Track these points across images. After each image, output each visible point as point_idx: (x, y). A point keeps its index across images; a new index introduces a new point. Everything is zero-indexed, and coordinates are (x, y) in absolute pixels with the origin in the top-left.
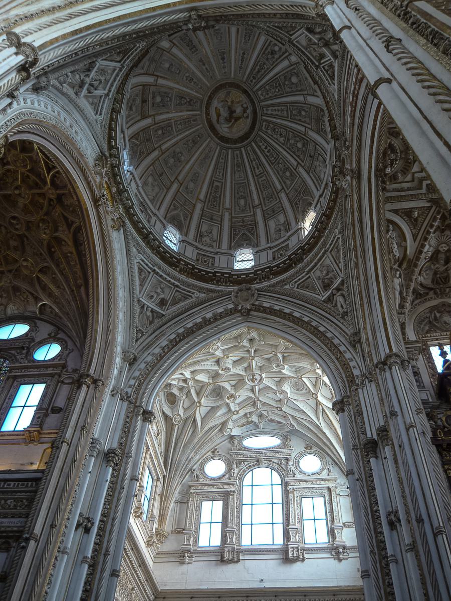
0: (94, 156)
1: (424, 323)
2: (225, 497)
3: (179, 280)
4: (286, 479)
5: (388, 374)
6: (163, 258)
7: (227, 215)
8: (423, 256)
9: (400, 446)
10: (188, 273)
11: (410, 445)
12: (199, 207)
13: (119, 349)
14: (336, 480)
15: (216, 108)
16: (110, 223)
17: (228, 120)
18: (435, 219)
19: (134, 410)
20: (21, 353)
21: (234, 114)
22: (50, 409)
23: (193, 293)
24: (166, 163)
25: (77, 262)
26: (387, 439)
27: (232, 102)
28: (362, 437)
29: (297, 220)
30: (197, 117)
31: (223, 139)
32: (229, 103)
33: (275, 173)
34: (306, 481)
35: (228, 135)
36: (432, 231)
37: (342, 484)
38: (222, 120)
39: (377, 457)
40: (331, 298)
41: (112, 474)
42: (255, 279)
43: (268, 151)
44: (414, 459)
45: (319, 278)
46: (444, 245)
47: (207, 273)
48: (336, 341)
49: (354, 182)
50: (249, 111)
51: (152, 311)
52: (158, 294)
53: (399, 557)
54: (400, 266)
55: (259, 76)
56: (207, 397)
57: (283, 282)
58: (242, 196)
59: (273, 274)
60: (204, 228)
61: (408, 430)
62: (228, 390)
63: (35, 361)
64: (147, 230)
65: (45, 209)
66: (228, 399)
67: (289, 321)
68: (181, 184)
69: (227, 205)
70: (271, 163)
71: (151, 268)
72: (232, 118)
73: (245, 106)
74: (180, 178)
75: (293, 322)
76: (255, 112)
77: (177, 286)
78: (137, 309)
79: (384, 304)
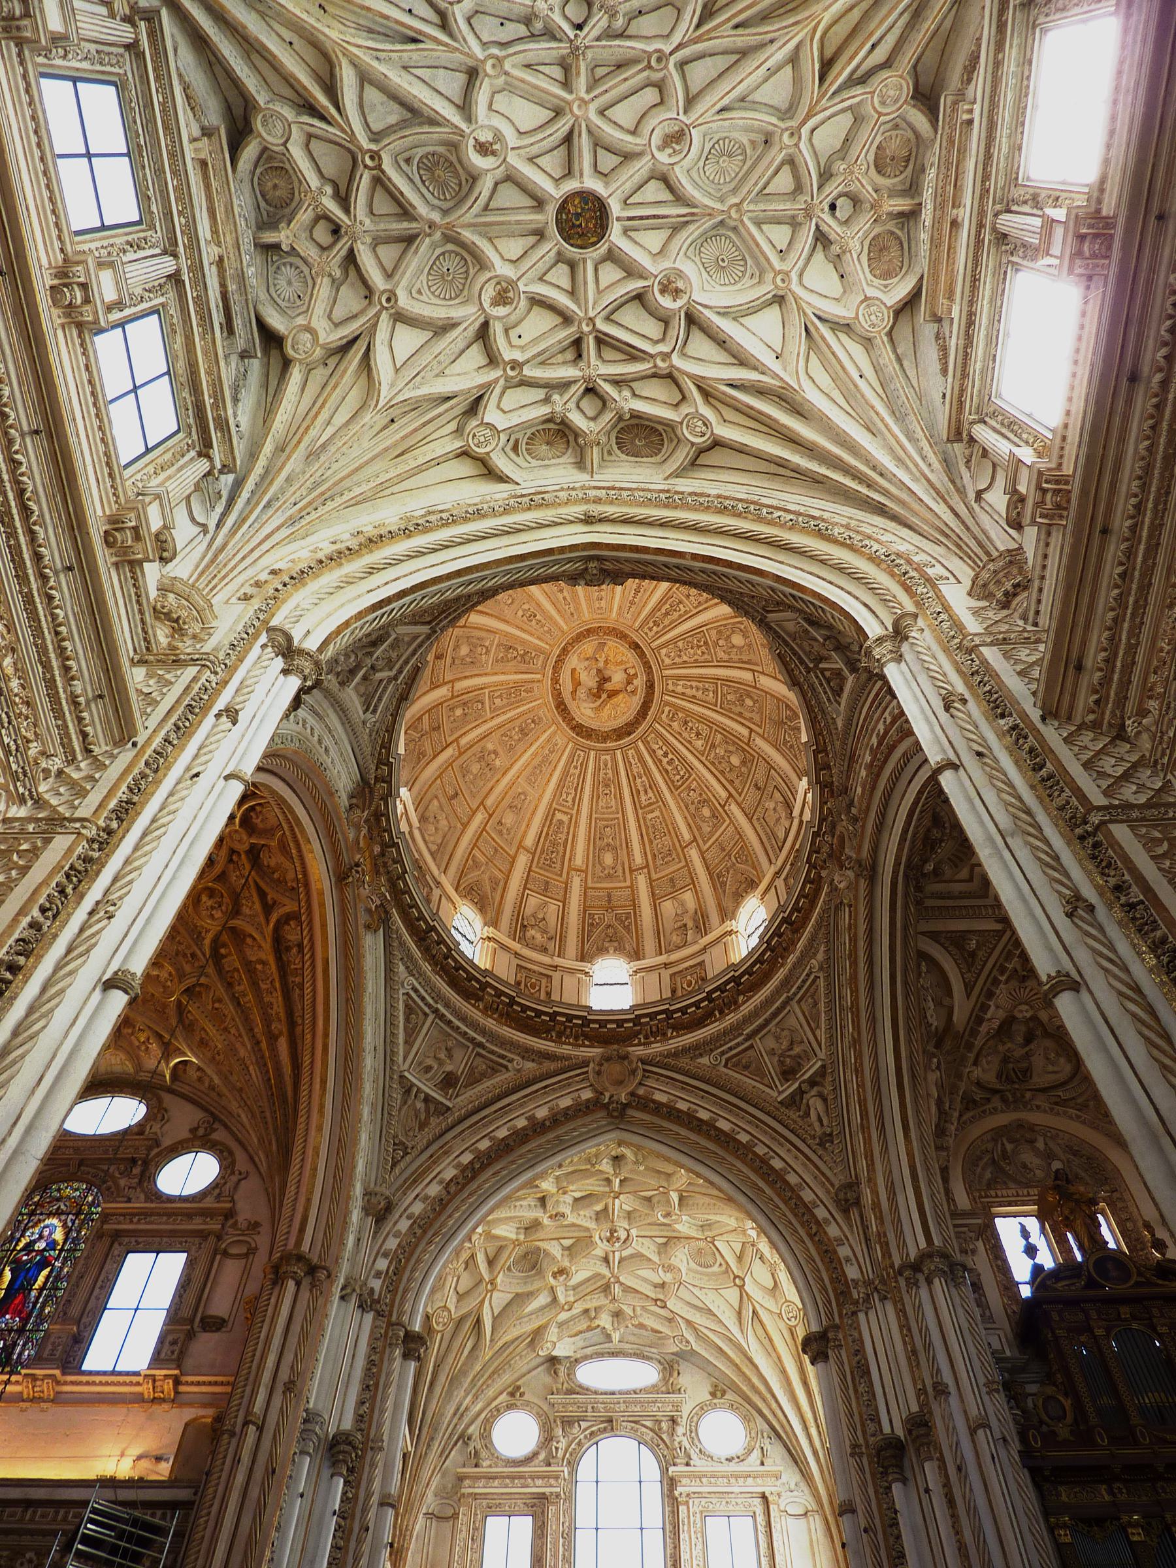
0: (350, 786)
1: (981, 1164)
2: (538, 1507)
4: (671, 1469)
5: (924, 1293)
6: (453, 983)
7: (576, 883)
8: (983, 1029)
9: (959, 1469)
10: (501, 1015)
11: (980, 1466)
12: (522, 860)
13: (358, 1189)
14: (778, 1476)
15: (573, 671)
16: (363, 918)
19: (386, 1332)
20: (127, 1173)
21: (608, 686)
22: (198, 1319)
23: (511, 1061)
24: (465, 771)
25: (277, 985)
26: (928, 1444)
27: (606, 662)
28: (871, 1427)
30: (536, 685)
31: (579, 729)
32: (601, 665)
33: (680, 808)
35: (593, 725)
36: (1003, 978)
37: (792, 1487)
38: (582, 692)
39: (904, 1481)
40: (798, 1098)
41: (344, 1493)
42: (636, 1035)
43: (670, 762)
44: (990, 1501)
45: (772, 1053)
46: (1025, 1007)
47: (539, 1013)
48: (807, 1196)
49: (863, 884)
51: (427, 1099)
52: (441, 1063)
54: (937, 1046)
55: (666, 622)
56: (509, 1269)
57: (696, 1050)
58: (608, 845)
59: (674, 1028)
62: (554, 1258)
63: (159, 1196)
64: (426, 922)
66: (555, 1275)
67: (708, 1137)
68: (491, 816)
69: (579, 861)
70: (673, 787)
71: (429, 1006)
72: (602, 690)
73: (632, 672)
74: (489, 802)
76: (650, 686)
77: (481, 1045)
78: (397, 1096)
79: (913, 1134)
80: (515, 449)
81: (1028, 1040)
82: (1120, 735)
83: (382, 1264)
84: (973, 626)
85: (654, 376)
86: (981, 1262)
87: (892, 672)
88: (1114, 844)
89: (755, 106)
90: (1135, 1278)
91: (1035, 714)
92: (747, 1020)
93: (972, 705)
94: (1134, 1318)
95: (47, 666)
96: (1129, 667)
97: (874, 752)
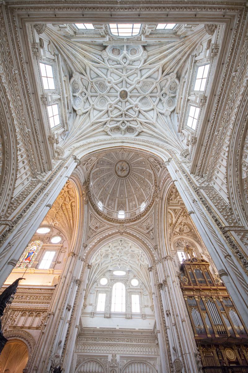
0: (83, 182)
3: (102, 221)
6: (98, 213)
7: (117, 199)
8: (177, 223)
12: (109, 195)
17: (121, 170)
18: (182, 213)
29: (139, 205)
31: (118, 176)
34: (133, 289)
39: (162, 290)
48: (150, 247)
49: (161, 201)
50: (128, 169)
51: (93, 230)
53: (170, 327)
54: (170, 226)
57: (134, 225)
60: (110, 202)
61: (173, 283)
65: (63, 194)
69: (117, 196)
72: (122, 170)
75: (136, 238)
76: (130, 170)
80: (111, 131)
81: (184, 226)
82: (202, 177)
83: (85, 254)
84: (180, 160)
85: (134, 120)
86: (175, 258)
87: (167, 167)
88: (201, 192)
89: (152, 78)
90: (198, 261)
91: (189, 173)
92: (142, 221)
93: (180, 172)
94: (198, 267)
95: (38, 157)
96: (204, 167)
97: (163, 181)
